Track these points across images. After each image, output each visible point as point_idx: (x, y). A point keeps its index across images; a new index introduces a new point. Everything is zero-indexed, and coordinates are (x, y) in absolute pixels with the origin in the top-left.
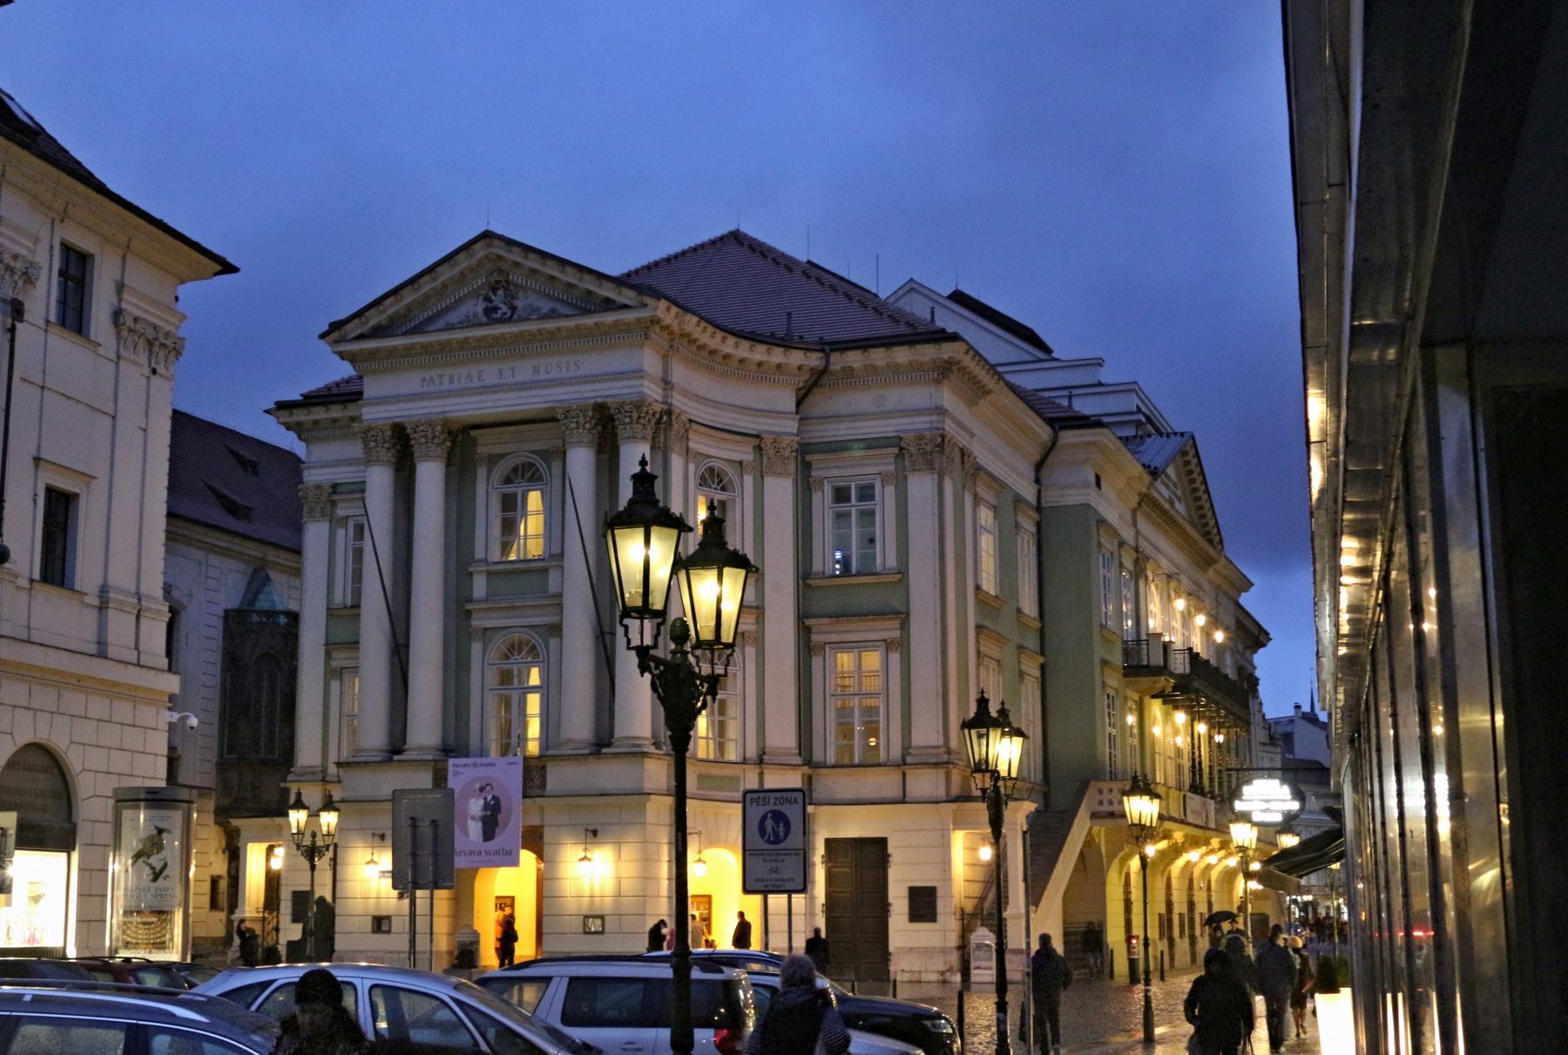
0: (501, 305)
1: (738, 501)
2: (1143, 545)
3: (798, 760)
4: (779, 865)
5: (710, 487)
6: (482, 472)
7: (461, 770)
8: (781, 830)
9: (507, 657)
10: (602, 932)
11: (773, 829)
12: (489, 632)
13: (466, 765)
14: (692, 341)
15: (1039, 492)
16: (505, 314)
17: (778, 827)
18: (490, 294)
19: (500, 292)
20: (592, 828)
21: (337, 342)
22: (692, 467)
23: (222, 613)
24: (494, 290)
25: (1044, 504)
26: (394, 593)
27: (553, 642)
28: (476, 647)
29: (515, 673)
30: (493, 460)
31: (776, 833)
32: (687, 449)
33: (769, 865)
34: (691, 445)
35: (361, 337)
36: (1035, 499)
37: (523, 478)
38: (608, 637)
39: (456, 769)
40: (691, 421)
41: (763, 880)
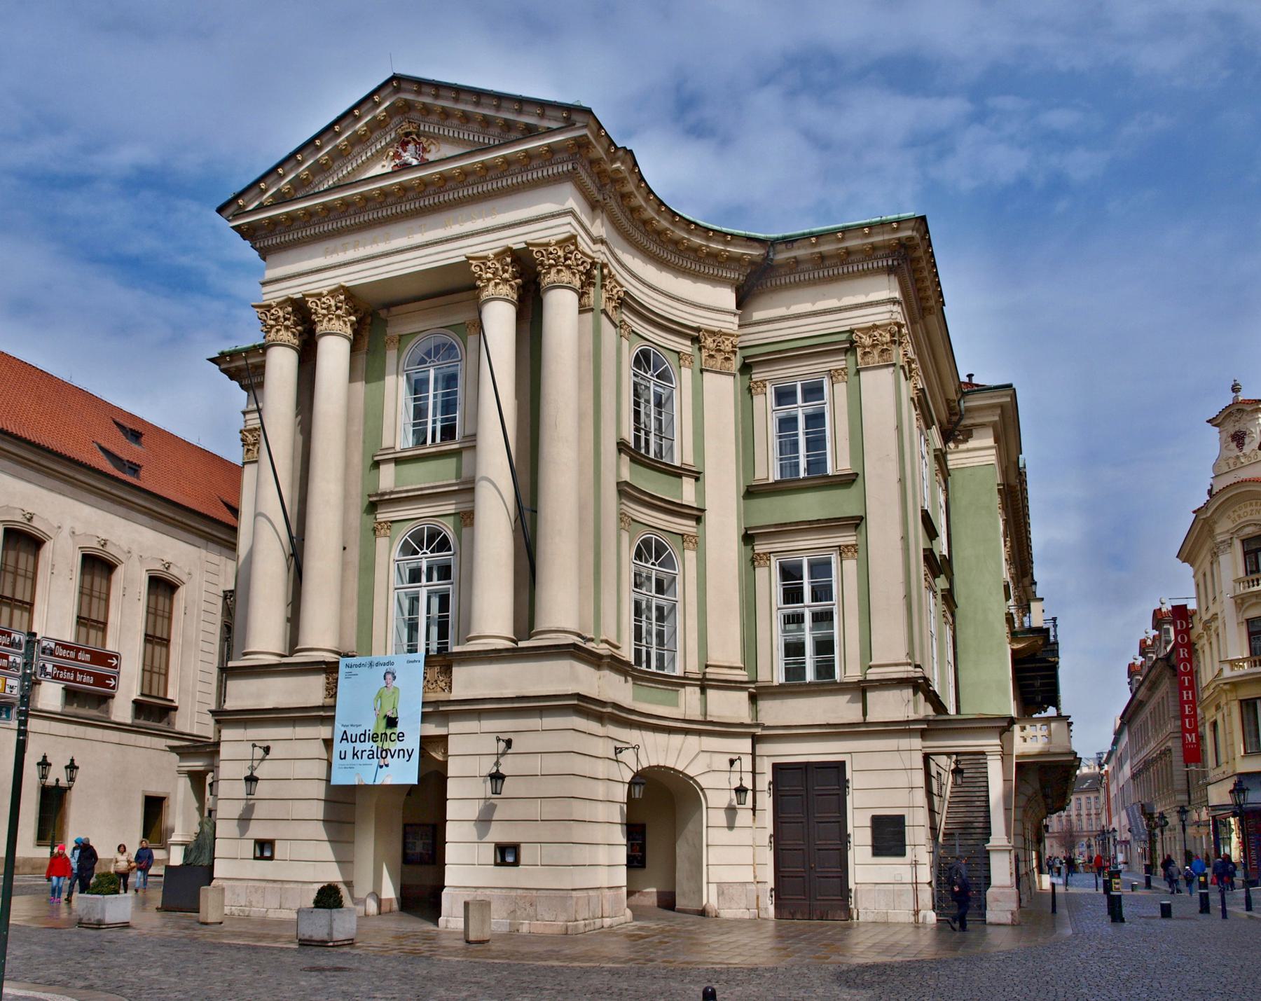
7: (354, 670)
10: (516, 863)
12: (395, 525)
13: (360, 665)
20: (506, 737)
22: (625, 343)
27: (465, 531)
39: (348, 670)
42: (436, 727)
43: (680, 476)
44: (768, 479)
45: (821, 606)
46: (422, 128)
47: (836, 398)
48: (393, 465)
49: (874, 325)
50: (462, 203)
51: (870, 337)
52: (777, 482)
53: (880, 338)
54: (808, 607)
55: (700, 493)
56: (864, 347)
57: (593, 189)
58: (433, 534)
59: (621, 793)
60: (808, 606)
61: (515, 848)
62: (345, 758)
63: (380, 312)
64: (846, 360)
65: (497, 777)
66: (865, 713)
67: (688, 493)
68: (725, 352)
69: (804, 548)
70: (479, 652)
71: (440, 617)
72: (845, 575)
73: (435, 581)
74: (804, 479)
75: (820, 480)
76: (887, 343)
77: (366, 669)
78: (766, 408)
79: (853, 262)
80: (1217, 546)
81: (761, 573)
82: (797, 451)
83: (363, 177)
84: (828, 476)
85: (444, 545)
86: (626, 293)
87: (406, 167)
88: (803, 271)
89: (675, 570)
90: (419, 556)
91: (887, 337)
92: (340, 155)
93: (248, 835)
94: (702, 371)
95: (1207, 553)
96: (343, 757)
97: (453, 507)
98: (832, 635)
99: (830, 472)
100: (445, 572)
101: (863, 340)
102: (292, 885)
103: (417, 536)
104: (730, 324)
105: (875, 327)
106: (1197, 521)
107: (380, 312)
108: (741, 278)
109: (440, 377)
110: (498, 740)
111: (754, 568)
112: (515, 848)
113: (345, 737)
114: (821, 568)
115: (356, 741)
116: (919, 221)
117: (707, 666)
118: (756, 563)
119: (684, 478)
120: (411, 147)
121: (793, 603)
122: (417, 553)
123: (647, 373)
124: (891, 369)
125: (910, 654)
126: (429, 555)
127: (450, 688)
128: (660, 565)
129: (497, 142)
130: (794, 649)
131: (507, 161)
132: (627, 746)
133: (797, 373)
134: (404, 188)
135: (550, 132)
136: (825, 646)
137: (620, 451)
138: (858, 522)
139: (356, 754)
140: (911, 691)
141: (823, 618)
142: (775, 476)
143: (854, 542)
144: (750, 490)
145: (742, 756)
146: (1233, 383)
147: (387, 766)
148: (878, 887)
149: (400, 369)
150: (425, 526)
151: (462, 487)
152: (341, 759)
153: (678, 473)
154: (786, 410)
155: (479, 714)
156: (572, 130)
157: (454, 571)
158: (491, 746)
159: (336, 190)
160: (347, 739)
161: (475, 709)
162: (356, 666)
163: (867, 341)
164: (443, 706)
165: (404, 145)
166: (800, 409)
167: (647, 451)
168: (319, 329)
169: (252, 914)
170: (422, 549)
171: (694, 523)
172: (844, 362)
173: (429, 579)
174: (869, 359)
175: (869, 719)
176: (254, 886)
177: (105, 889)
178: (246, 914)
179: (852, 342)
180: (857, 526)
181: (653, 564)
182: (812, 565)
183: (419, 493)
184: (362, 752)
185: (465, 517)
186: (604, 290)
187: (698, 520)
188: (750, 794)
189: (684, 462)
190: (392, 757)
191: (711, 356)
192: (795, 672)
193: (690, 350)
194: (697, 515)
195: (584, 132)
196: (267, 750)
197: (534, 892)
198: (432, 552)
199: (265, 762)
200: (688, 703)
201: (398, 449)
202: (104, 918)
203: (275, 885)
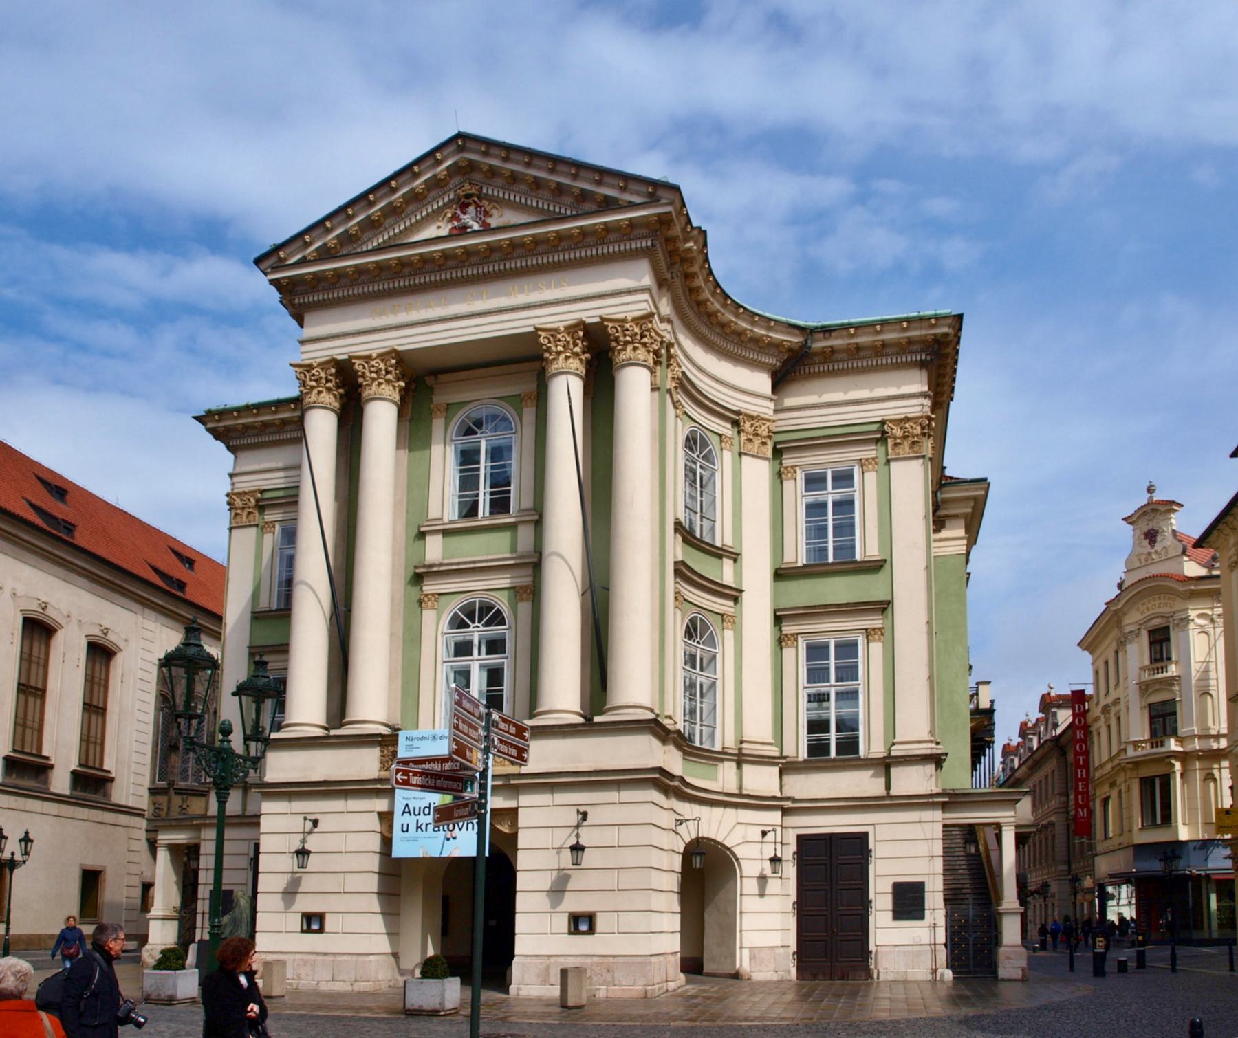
6: (438, 425)
12: (443, 598)
26: (336, 547)
30: (449, 409)
42: (504, 799)
43: (720, 557)
44: (796, 562)
46: (484, 191)
47: (866, 488)
49: (906, 417)
50: (529, 271)
51: (901, 428)
52: (805, 566)
53: (911, 430)
54: (834, 686)
55: (738, 575)
56: (895, 438)
57: (663, 265)
60: (832, 687)
62: (407, 831)
63: (426, 378)
64: (876, 450)
67: (726, 573)
68: (761, 437)
69: (832, 630)
70: (553, 726)
71: (488, 691)
72: (871, 657)
73: (483, 656)
74: (833, 564)
75: (852, 567)
76: (917, 436)
77: (429, 742)
78: (796, 494)
79: (887, 355)
80: (1125, 636)
81: (788, 653)
82: (826, 536)
83: (406, 241)
84: (856, 562)
85: (498, 619)
86: (683, 373)
87: (462, 231)
88: (837, 361)
89: (715, 648)
91: (918, 430)
92: (393, 212)
93: (294, 908)
94: (740, 454)
95: (1111, 643)
96: (405, 829)
97: (508, 581)
98: (857, 714)
99: (858, 557)
101: (894, 431)
102: (345, 958)
104: (765, 408)
105: (907, 419)
106: (1107, 612)
107: (426, 378)
109: (489, 448)
111: (781, 649)
113: (407, 810)
114: (847, 649)
115: (419, 814)
116: (957, 318)
118: (783, 644)
119: (724, 559)
120: (471, 209)
121: (824, 682)
122: (468, 626)
123: (693, 453)
124: (921, 461)
125: (932, 733)
126: (482, 628)
128: (704, 644)
129: (574, 213)
131: (584, 232)
133: (827, 461)
134: (468, 252)
135: (632, 206)
138: (885, 606)
139: (420, 827)
140: (933, 766)
141: (850, 696)
142: (802, 560)
143: (880, 626)
144: (779, 572)
146: (1148, 484)
147: (454, 838)
149: (448, 439)
150: (477, 600)
151: (518, 561)
152: (403, 831)
153: (718, 553)
154: (816, 496)
155: (552, 788)
156: (656, 206)
159: (390, 249)
160: (409, 812)
161: (551, 783)
162: (418, 739)
163: (898, 432)
164: (514, 779)
165: (464, 207)
166: (830, 496)
168: (366, 393)
169: (300, 987)
170: (474, 622)
171: (731, 603)
172: (875, 452)
174: (899, 450)
176: (302, 959)
177: (174, 965)
178: (295, 987)
179: (884, 433)
180: (884, 610)
181: (698, 643)
182: (838, 646)
184: (427, 825)
185: (521, 591)
186: (669, 370)
187: (736, 600)
189: (725, 543)
190: (460, 829)
191: (750, 440)
193: (730, 432)
194: (734, 595)
195: (669, 209)
199: (313, 835)
200: (725, 778)
201: (446, 520)
202: (176, 993)
203: (326, 958)
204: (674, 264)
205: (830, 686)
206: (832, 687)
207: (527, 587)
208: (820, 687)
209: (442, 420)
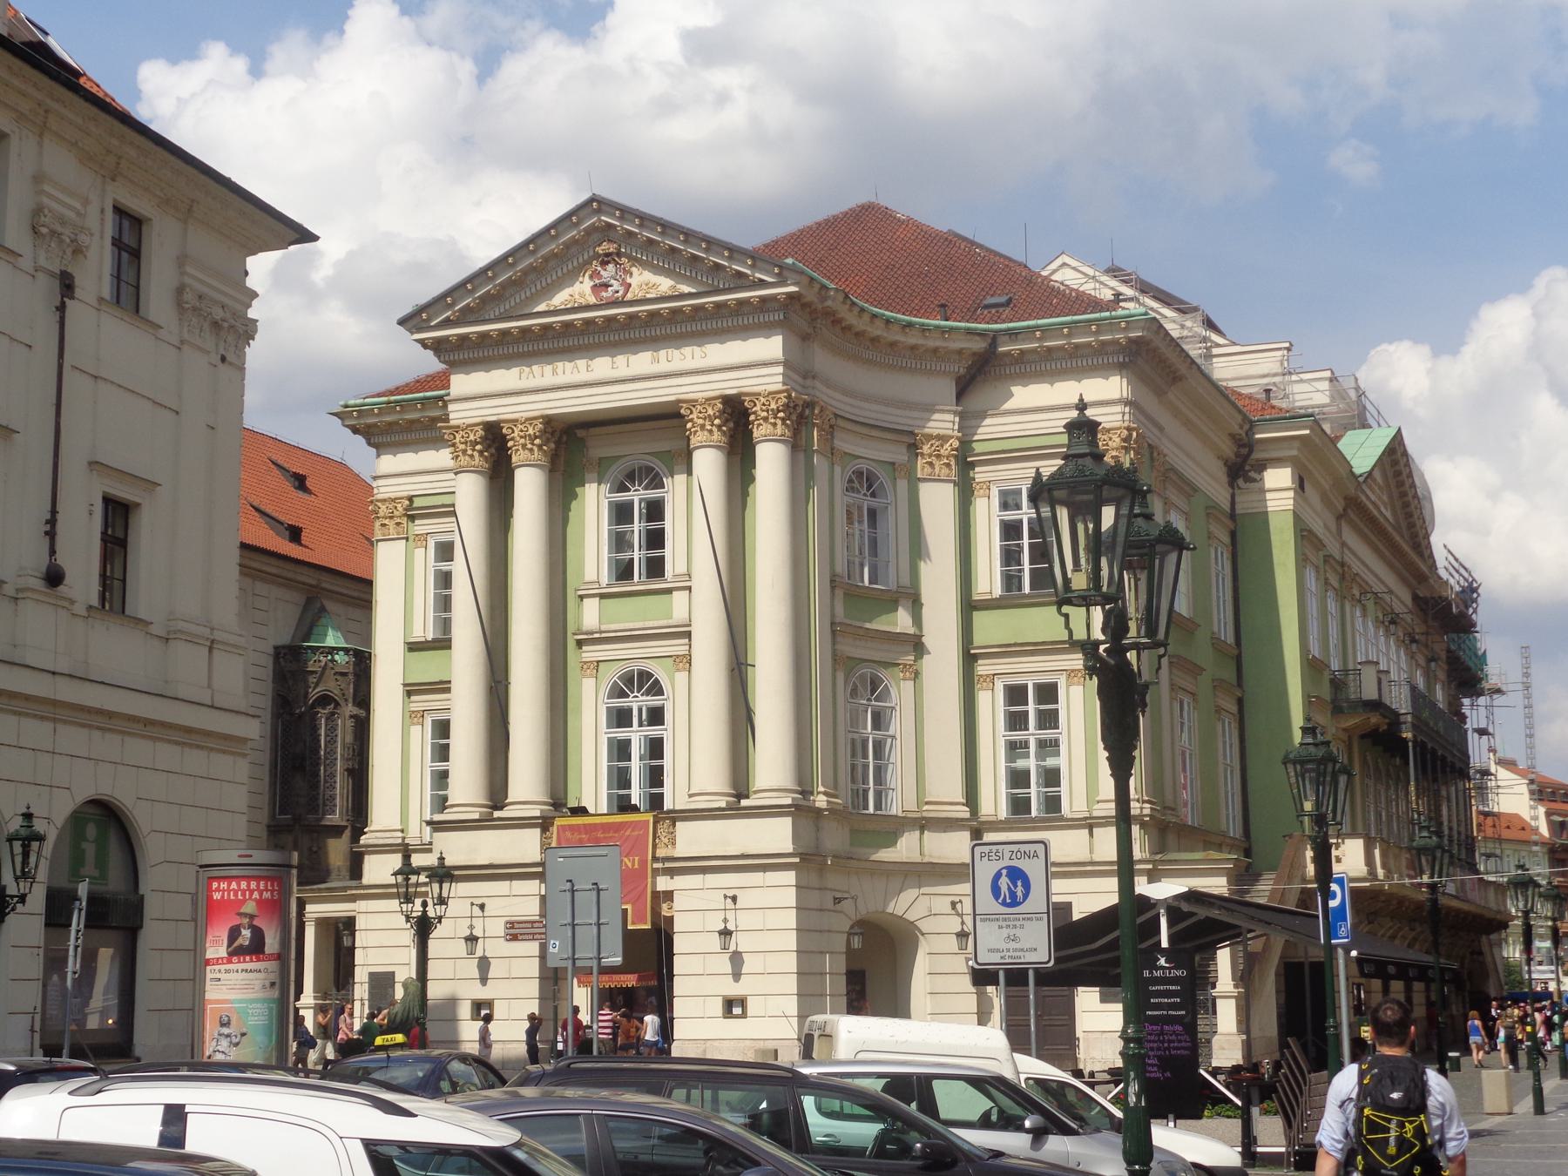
0: (613, 282)
1: (891, 510)
2: (1349, 558)
3: (963, 812)
4: (1018, 932)
5: (859, 492)
8: (1019, 891)
9: (623, 694)
10: (744, 1015)
11: (1009, 888)
14: (837, 322)
15: (1233, 496)
16: (617, 292)
17: (1016, 886)
18: (599, 269)
19: (611, 267)
21: (420, 330)
22: (838, 469)
23: (271, 651)
24: (604, 264)
25: (1239, 511)
28: (588, 684)
29: (635, 713)
31: (1013, 895)
32: (832, 449)
33: (1005, 932)
34: (837, 443)
35: (447, 323)
36: (1229, 505)
37: (639, 486)
38: (743, 667)
40: (836, 416)
41: (998, 951)
45: (1048, 734)
48: (598, 599)
54: (1033, 735)
55: (917, 620)
58: (645, 676)
59: (840, 943)
60: (1032, 734)
61: (742, 1002)
65: (726, 933)
66: (1091, 851)
85: (657, 689)
90: (630, 699)
100: (656, 716)
103: (628, 679)
108: (961, 370)
110: (726, 897)
112: (742, 1002)
114: (1048, 693)
117: (927, 803)
122: (628, 696)
127: (674, 844)
128: (876, 700)
130: (1018, 779)
132: (846, 895)
136: (1052, 777)
137: (833, 588)
141: (1049, 747)
142: (998, 591)
145: (961, 898)
148: (1105, 1035)
157: (668, 716)
158: (717, 900)
167: (863, 581)
173: (641, 725)
175: (1097, 858)
183: (628, 633)
188: (971, 938)
189: (901, 584)
192: (1019, 806)
196: (482, 907)
197: (762, 1042)
198: (642, 695)
204: (816, 319)
205: (1030, 735)
206: (1032, 734)
207: (684, 656)
208: (1017, 736)
209: (596, 475)
